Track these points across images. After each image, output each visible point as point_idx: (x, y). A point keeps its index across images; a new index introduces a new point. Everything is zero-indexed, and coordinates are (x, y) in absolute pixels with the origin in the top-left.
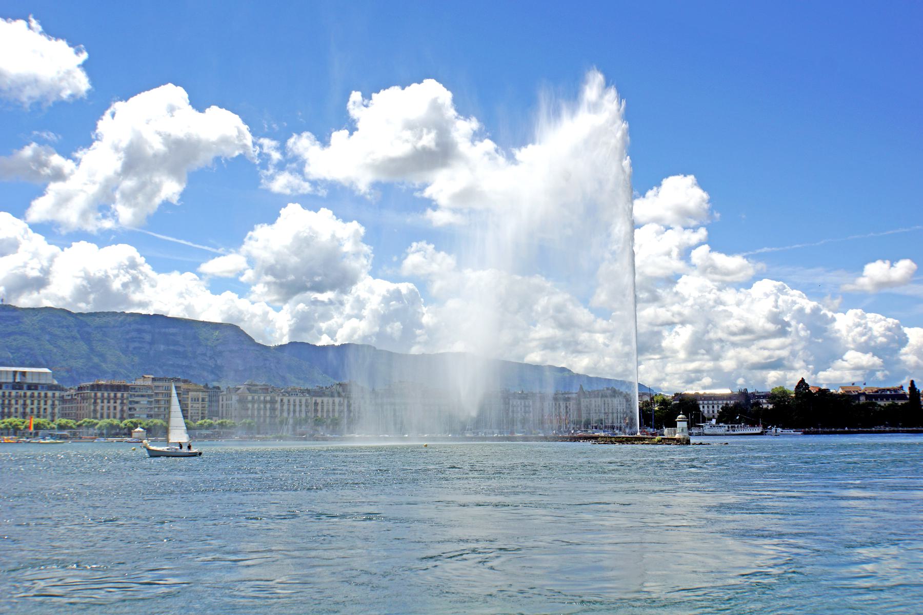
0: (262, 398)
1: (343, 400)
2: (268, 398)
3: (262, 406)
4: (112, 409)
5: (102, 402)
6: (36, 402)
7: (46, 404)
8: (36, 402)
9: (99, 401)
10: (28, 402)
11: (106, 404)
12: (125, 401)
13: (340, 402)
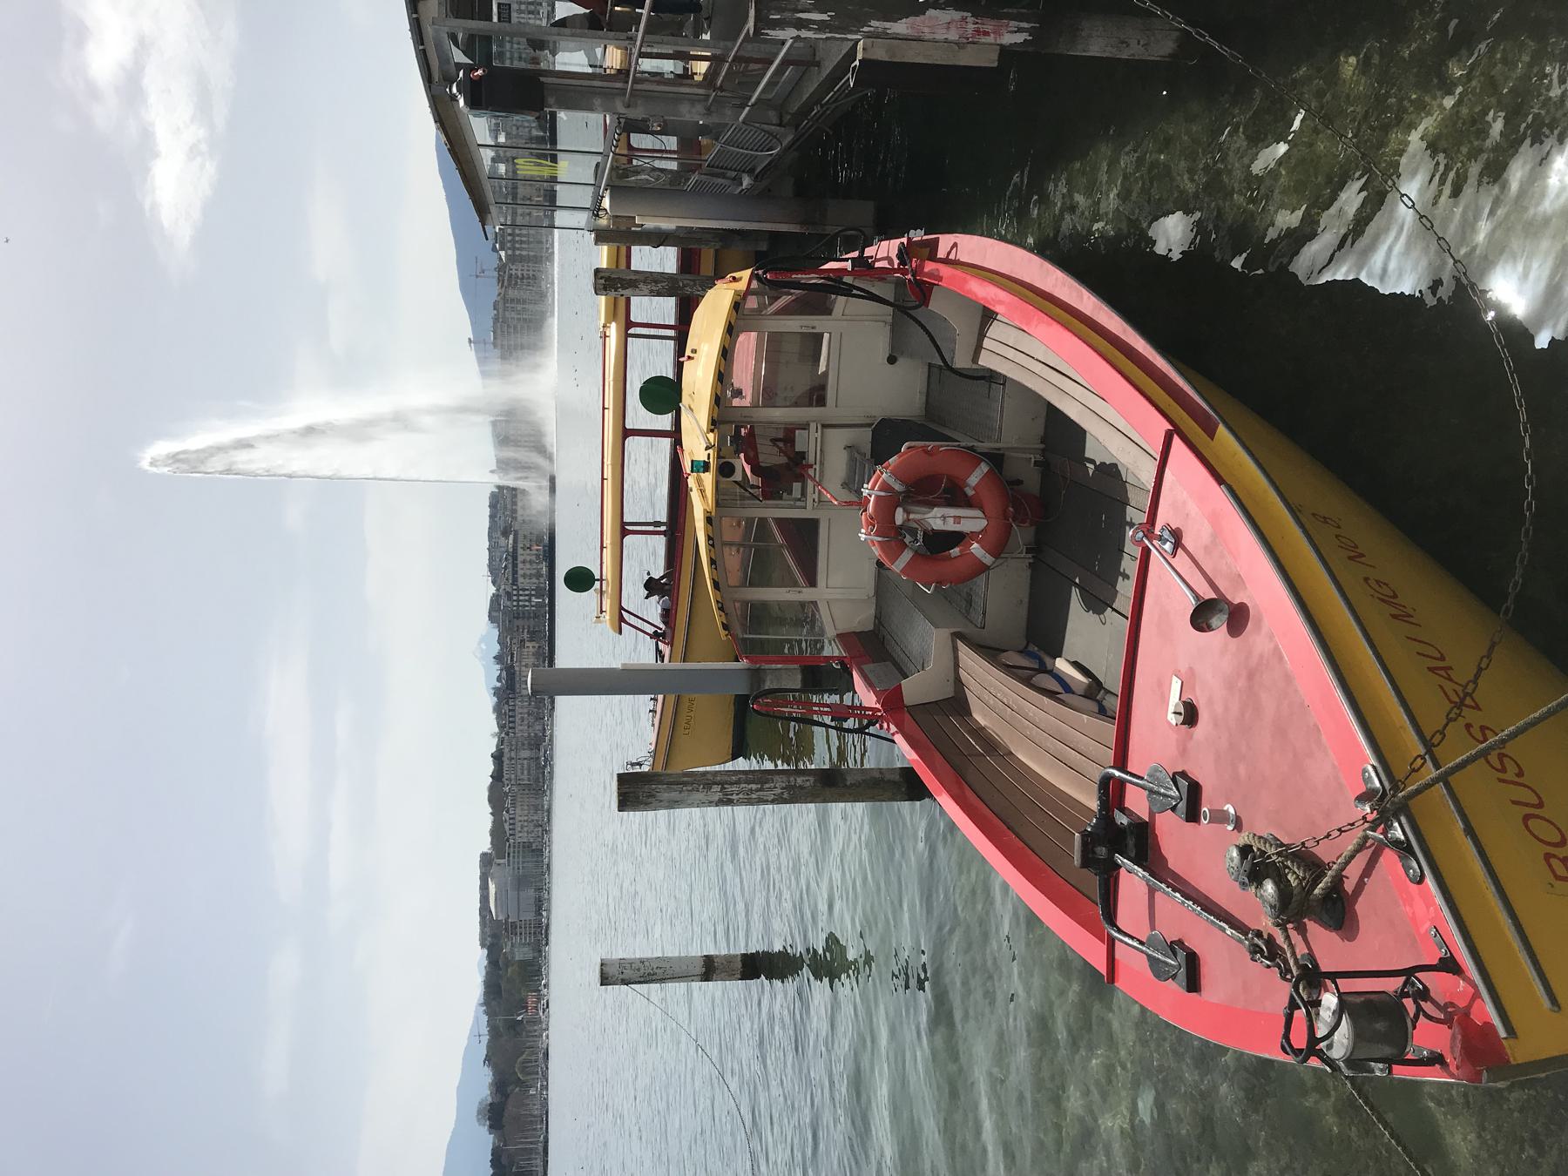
0: (509, 238)
3: (517, 238)
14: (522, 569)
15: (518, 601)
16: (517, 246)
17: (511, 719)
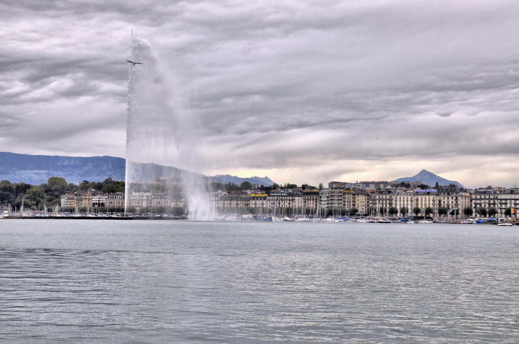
1: (436, 198)
2: (388, 197)
3: (384, 201)
6: (283, 201)
7: (287, 202)
8: (283, 201)
9: (307, 200)
11: (309, 202)
12: (317, 200)
13: (434, 198)
14: (227, 203)
16: (381, 201)
17: (159, 197)
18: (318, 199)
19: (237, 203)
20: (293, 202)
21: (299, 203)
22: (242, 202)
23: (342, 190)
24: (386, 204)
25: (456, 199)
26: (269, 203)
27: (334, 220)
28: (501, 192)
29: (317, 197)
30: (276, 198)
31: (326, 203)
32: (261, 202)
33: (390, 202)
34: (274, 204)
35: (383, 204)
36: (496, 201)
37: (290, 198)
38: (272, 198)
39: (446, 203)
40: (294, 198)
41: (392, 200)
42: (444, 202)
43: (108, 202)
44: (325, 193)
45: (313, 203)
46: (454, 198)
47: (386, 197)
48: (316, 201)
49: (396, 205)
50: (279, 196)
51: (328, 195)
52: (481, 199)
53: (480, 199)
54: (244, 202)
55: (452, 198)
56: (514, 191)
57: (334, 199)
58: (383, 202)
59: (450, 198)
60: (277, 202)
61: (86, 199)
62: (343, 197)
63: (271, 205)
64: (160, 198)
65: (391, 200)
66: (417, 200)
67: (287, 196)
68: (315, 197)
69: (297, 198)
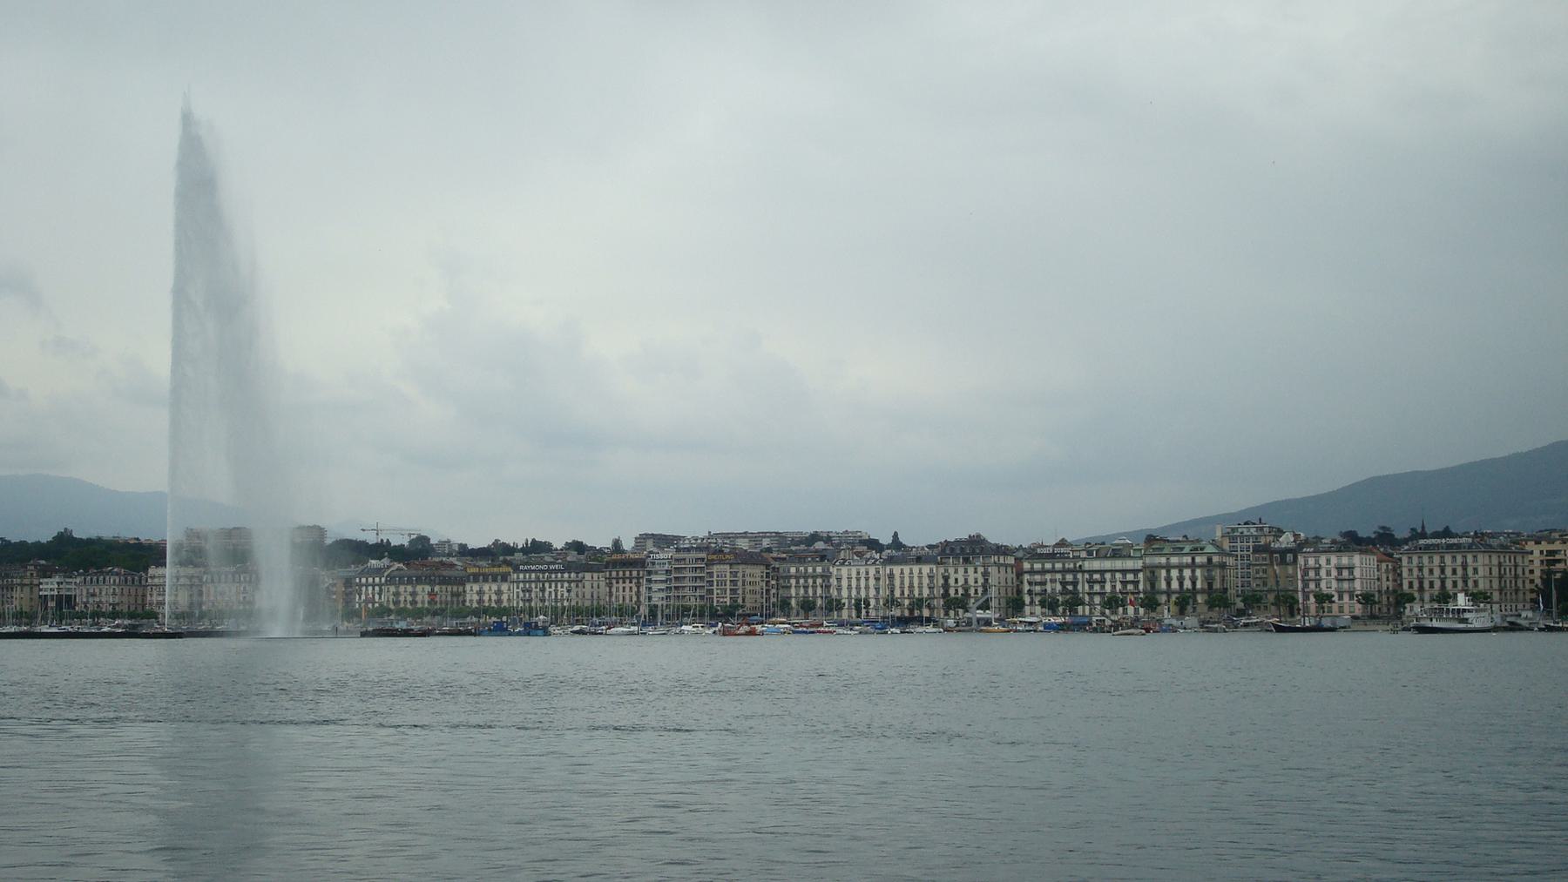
0: (810, 570)
1: (937, 570)
3: (810, 581)
4: (627, 590)
5: (617, 583)
7: (562, 587)
9: (614, 581)
10: (547, 585)
11: (621, 585)
12: (641, 581)
13: (931, 570)
14: (405, 591)
15: (367, 585)
16: (802, 581)
17: (223, 577)
18: (642, 578)
19: (433, 590)
20: (577, 586)
21: (592, 587)
22: (444, 587)
23: (703, 555)
24: (814, 587)
25: (986, 574)
26: (516, 590)
27: (700, 628)
28: (1090, 553)
29: (641, 572)
30: (533, 575)
31: (663, 586)
32: (494, 587)
33: (824, 581)
34: (530, 591)
35: (806, 588)
36: (1079, 576)
37: (570, 577)
38: (525, 577)
39: (961, 582)
40: (580, 575)
41: (828, 577)
42: (956, 580)
43: (85, 593)
44: (659, 561)
45: (631, 588)
46: (981, 570)
47: (814, 570)
48: (639, 582)
49: (839, 589)
50: (543, 572)
51: (666, 567)
52: (1043, 572)
53: (1183, 567)
54: (449, 588)
55: (976, 572)
56: (1120, 550)
57: (684, 577)
58: (806, 581)
59: (971, 570)
60: (536, 587)
61: (22, 585)
62: (706, 571)
63: (521, 595)
64: (226, 582)
65: (826, 576)
66: (891, 576)
67: (562, 572)
68: (635, 574)
69: (588, 576)
